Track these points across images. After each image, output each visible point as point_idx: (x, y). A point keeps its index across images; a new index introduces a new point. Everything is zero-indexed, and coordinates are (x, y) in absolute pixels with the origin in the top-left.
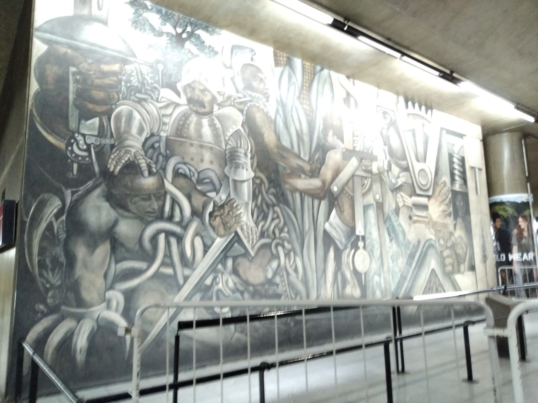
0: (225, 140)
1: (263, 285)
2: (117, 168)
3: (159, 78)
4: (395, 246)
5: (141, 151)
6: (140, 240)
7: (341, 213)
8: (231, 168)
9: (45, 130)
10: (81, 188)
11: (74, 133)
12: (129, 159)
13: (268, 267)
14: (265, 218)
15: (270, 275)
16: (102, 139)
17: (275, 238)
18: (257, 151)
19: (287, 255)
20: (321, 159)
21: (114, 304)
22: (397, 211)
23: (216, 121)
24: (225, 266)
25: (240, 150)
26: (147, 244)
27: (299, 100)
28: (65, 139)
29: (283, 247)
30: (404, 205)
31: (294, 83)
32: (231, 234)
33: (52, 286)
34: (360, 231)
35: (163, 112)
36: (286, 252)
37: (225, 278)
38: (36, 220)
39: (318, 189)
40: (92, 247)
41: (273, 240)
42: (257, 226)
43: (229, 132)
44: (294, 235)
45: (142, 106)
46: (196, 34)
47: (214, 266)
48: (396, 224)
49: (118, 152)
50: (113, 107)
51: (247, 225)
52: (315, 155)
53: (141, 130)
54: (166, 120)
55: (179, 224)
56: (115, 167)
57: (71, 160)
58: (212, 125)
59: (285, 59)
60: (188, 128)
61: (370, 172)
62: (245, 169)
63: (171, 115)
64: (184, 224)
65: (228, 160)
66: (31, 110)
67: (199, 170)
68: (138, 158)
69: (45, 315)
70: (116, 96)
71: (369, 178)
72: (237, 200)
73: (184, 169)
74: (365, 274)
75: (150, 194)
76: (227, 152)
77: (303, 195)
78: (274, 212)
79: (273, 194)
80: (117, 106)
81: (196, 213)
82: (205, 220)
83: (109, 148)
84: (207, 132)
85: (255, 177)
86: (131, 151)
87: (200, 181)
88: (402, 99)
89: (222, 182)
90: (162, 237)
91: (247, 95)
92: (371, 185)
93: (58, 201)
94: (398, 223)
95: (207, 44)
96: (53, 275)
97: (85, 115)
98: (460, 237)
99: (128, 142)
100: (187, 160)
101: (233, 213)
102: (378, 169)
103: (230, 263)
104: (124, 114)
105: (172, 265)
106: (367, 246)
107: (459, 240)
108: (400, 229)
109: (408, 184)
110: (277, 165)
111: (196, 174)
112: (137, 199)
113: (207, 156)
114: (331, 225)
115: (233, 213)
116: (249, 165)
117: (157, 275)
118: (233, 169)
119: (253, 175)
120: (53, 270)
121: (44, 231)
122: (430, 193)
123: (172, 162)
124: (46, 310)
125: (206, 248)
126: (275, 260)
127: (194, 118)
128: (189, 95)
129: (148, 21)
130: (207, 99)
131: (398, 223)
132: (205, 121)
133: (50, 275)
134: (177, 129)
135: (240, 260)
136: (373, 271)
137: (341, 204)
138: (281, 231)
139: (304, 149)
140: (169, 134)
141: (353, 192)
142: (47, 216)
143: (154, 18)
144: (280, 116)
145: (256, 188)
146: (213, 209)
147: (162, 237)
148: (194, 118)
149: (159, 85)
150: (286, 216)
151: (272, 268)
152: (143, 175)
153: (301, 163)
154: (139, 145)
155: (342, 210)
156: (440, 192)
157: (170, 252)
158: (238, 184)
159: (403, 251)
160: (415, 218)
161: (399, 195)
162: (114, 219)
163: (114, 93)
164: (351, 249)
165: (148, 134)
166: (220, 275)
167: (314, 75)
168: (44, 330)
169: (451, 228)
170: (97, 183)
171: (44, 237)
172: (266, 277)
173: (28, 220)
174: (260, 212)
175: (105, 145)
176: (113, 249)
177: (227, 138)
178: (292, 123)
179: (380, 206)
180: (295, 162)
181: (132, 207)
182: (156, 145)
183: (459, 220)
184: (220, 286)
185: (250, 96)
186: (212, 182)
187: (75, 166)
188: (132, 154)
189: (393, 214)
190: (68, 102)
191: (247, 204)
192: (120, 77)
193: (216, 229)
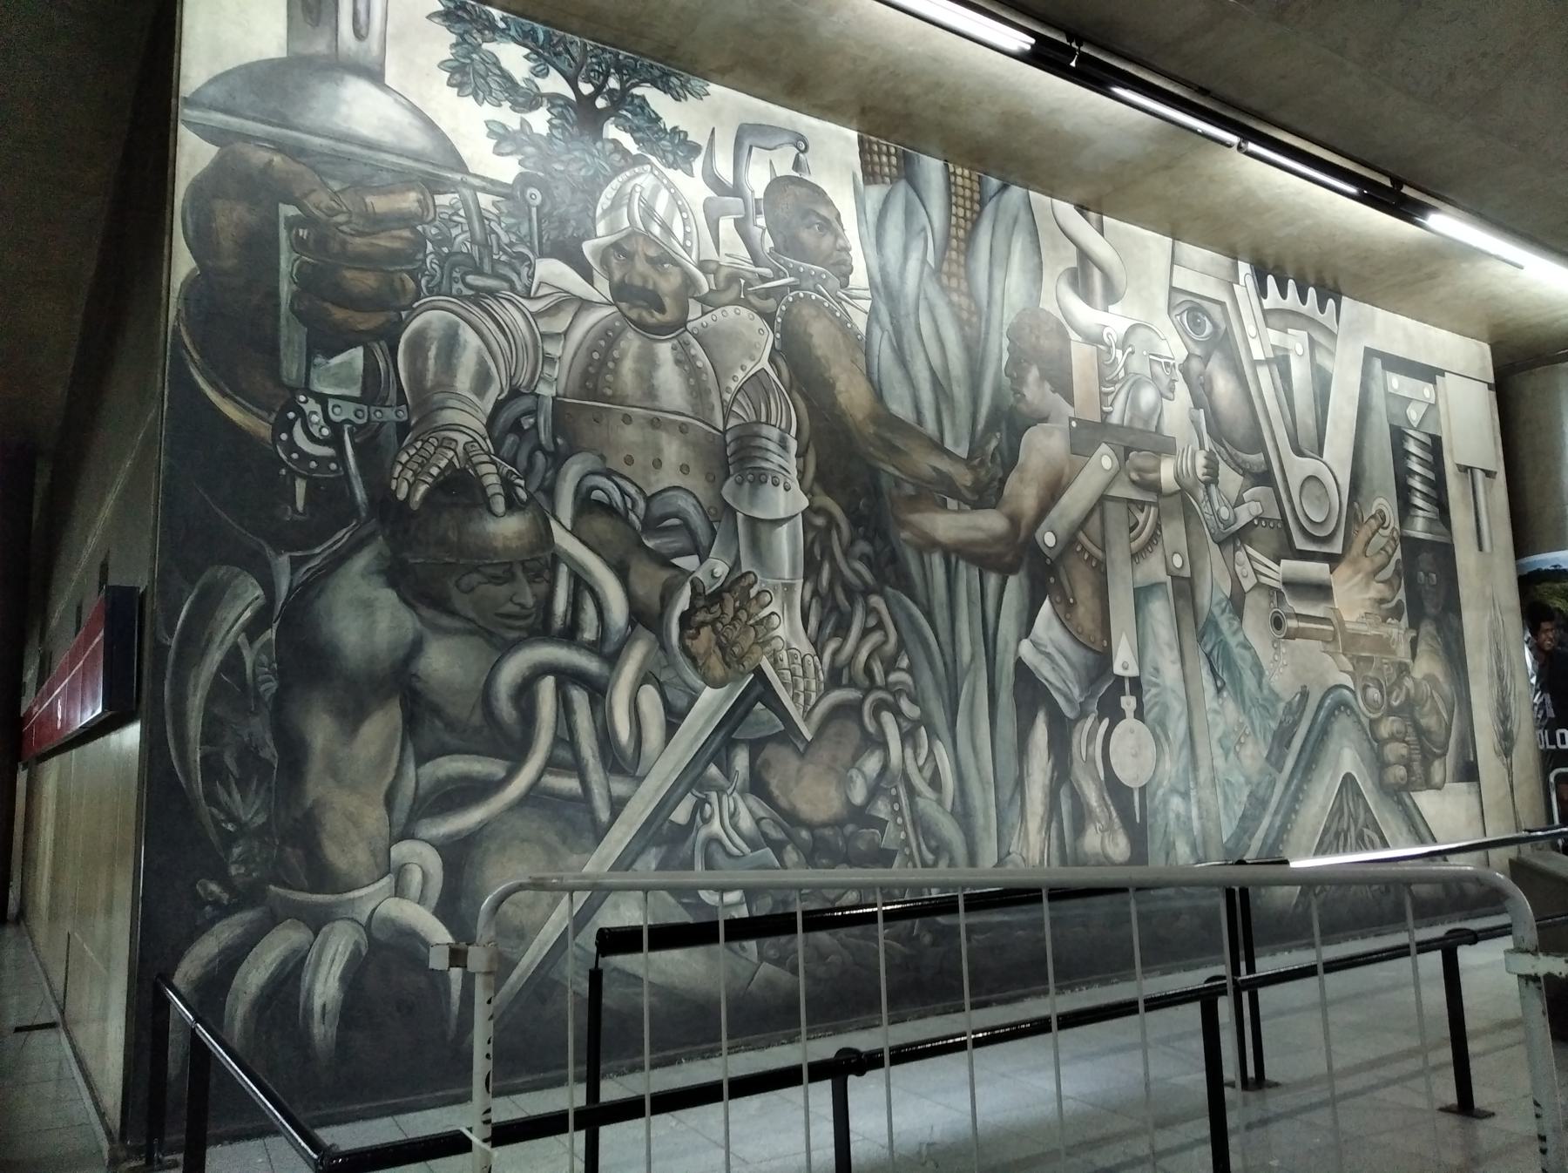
0: (722, 401)
1: (838, 823)
2: (416, 490)
3: (530, 228)
4: (1230, 706)
5: (484, 439)
6: (487, 696)
8: (740, 484)
9: (213, 384)
10: (318, 550)
11: (294, 391)
12: (450, 461)
13: (854, 772)
14: (842, 630)
15: (859, 796)
16: (373, 409)
17: (873, 686)
18: (815, 432)
19: (908, 737)
20: (1006, 454)
21: (415, 877)
22: (1237, 603)
23: (697, 350)
24: (727, 770)
25: (765, 430)
26: (505, 709)
27: (939, 280)
28: (270, 410)
29: (897, 713)
30: (1259, 585)
31: (924, 229)
32: (744, 675)
34: (1124, 661)
35: (544, 326)
38: (194, 640)
39: (998, 539)
40: (352, 717)
41: (867, 692)
42: (820, 655)
44: (926, 678)
46: (633, 96)
47: (699, 769)
48: (1233, 642)
49: (419, 444)
50: (404, 314)
51: (789, 648)
52: (988, 442)
53: (482, 381)
54: (553, 349)
55: (594, 648)
56: (412, 487)
57: (290, 470)
58: (684, 360)
60: (615, 372)
61: (1154, 487)
62: (781, 486)
63: (566, 333)
64: (609, 648)
65: (730, 460)
66: (176, 331)
67: (649, 494)
68: (475, 460)
69: (225, 911)
70: (411, 285)
71: (1150, 504)
72: (759, 577)
73: (606, 490)
74: (1143, 789)
75: (511, 563)
76: (728, 438)
77: (953, 560)
78: (870, 611)
79: (864, 558)
81: (644, 617)
82: (669, 637)
83: (392, 432)
84: (669, 379)
86: (456, 441)
87: (653, 524)
88: (1244, 268)
90: (547, 685)
92: (1158, 526)
93: (255, 587)
94: (1240, 638)
97: (327, 341)
98: (1430, 678)
99: (449, 416)
100: (616, 463)
102: (1177, 478)
103: (741, 760)
104: (435, 333)
105: (577, 767)
106: (1146, 708)
107: (1426, 688)
108: (1247, 655)
109: (1268, 520)
110: (875, 473)
111: (641, 504)
112: (476, 577)
113: (672, 450)
114: (1035, 644)
115: (750, 617)
116: (794, 473)
117: (535, 797)
118: (747, 484)
119: (805, 503)
120: (243, 784)
121: (219, 670)
122: (1336, 548)
123: (573, 472)
124: (225, 897)
125: (674, 718)
126: (872, 752)
127: (632, 343)
128: (617, 276)
129: (497, 64)
130: (668, 284)
131: (1240, 638)
132: (665, 350)
133: (237, 797)
134: (586, 376)
135: (770, 751)
137: (1066, 583)
138: (890, 665)
139: (953, 424)
140: (561, 392)
141: (1104, 551)
142: (226, 627)
143: (513, 58)
144: (883, 330)
145: (813, 543)
146: (691, 603)
147: (547, 685)
148: (632, 343)
150: (904, 625)
151: (864, 776)
153: (944, 465)
154: (477, 424)
155: (1071, 601)
156: (1368, 543)
157: (571, 730)
158: (763, 529)
159: (1257, 723)
160: (1292, 623)
161: (1241, 555)
162: (410, 637)
163: (406, 276)
164: (1100, 719)
165: (502, 390)
166: (714, 796)
167: (982, 203)
168: (221, 953)
169: (1403, 652)
170: (364, 532)
171: (217, 691)
172: (848, 801)
173: (173, 643)
174: (826, 610)
175: (382, 424)
176: (411, 723)
177: (728, 397)
178: (917, 347)
179: (1184, 589)
180: (927, 463)
181: (460, 602)
182: (527, 423)
183: (1427, 628)
185: (794, 272)
186: (686, 526)
187: (301, 487)
188: (460, 449)
189: (1223, 611)
190: (278, 305)
191: (789, 588)
192: (420, 228)
193: (700, 663)
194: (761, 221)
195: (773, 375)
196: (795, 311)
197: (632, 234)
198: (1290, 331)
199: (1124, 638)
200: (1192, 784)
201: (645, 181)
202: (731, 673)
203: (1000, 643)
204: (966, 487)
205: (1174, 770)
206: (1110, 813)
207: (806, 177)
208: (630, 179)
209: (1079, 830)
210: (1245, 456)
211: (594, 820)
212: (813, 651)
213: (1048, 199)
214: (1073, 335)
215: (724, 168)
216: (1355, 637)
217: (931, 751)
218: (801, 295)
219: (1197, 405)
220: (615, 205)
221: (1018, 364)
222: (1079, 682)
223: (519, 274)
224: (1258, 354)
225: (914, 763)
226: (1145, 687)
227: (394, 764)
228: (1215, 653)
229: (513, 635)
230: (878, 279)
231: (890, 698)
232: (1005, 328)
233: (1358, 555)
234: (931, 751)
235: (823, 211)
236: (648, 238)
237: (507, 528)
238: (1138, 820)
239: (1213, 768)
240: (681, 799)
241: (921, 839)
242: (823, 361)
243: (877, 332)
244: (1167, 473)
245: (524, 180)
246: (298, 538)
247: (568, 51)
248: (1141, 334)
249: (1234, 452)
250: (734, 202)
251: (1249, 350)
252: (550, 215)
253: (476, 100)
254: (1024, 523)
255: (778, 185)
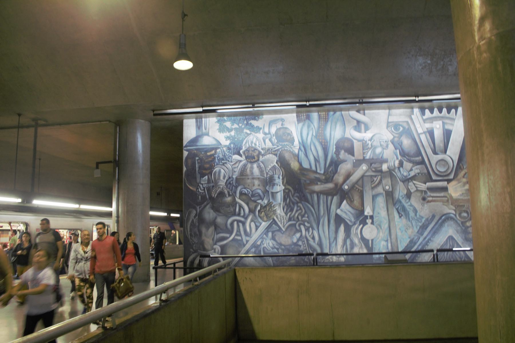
0: (266, 172)
1: (290, 245)
4: (404, 220)
7: (351, 203)
8: (270, 186)
9: (189, 185)
11: (198, 184)
12: (220, 190)
13: (294, 236)
14: (292, 210)
15: (295, 240)
19: (307, 229)
20: (334, 170)
21: (217, 250)
22: (409, 195)
24: (267, 236)
26: (229, 226)
30: (417, 190)
31: (313, 128)
32: (271, 220)
33: (195, 243)
34: (368, 211)
35: (234, 166)
36: (306, 228)
37: (267, 242)
38: (188, 219)
39: (331, 189)
40: (208, 228)
41: (297, 222)
43: (269, 168)
45: (224, 166)
47: (262, 236)
48: (406, 205)
51: (280, 215)
54: (235, 170)
55: (243, 217)
56: (215, 195)
58: (259, 167)
59: (305, 117)
60: (246, 171)
61: (381, 171)
64: (245, 216)
66: (184, 180)
69: (193, 253)
70: (214, 165)
72: (274, 202)
73: (245, 191)
74: (372, 240)
76: (267, 178)
77: (319, 195)
79: (297, 197)
80: (214, 169)
81: (252, 211)
84: (256, 171)
85: (285, 189)
87: (253, 195)
89: (265, 194)
90: (235, 223)
91: (279, 145)
94: (409, 204)
95: (255, 126)
96: (195, 239)
97: (203, 175)
101: (272, 210)
102: (388, 168)
103: (270, 234)
104: (217, 171)
105: (240, 235)
108: (412, 208)
110: (300, 180)
111: (251, 193)
113: (257, 182)
114: (341, 210)
115: (272, 210)
116: (281, 183)
117: (234, 239)
118: (271, 187)
119: (283, 188)
120: (195, 237)
121: (191, 222)
124: (193, 251)
125: (257, 228)
126: (298, 233)
127: (249, 165)
128: (246, 155)
129: (226, 126)
130: (255, 154)
131: (409, 204)
132: (255, 166)
133: (194, 239)
134: (241, 173)
135: (276, 233)
136: (380, 238)
138: (303, 216)
140: (237, 176)
141: (363, 187)
143: (228, 124)
144: (302, 151)
145: (285, 195)
146: (260, 208)
147: (235, 223)
148: (249, 165)
149: (232, 154)
150: (306, 209)
151: (296, 237)
152: (226, 196)
153: (317, 176)
154: (224, 184)
155: (352, 200)
157: (239, 229)
158: (275, 194)
159: (414, 224)
160: (431, 199)
161: (411, 184)
164: (360, 225)
167: (328, 119)
171: (191, 225)
172: (293, 242)
173: (186, 219)
175: (210, 186)
177: (267, 171)
180: (312, 176)
181: (222, 211)
182: (231, 182)
184: (265, 245)
185: (281, 145)
186: (259, 195)
187: (200, 197)
189: (403, 198)
190: (196, 172)
191: (280, 204)
193: (262, 218)
194: (274, 137)
195: (277, 165)
196: (282, 152)
197: (249, 147)
198: (434, 122)
199: (368, 207)
200: (389, 238)
201: (251, 137)
202: (268, 219)
203: (331, 211)
204: (323, 179)
205: (383, 235)
206: (362, 245)
207: (284, 126)
208: (248, 138)
209: (352, 248)
210: (414, 159)
211: (244, 244)
212: (285, 215)
213: (347, 112)
214: (355, 141)
215: (267, 130)
216: (457, 200)
217: (312, 233)
218: (283, 149)
219: (396, 149)
220: (246, 143)
221: (337, 152)
222: (354, 217)
223: (230, 159)
224: (420, 131)
225: (308, 235)
226: (374, 217)
227: (213, 235)
228: (400, 208)
229: (230, 215)
230: (301, 141)
231: (303, 223)
232: (334, 144)
233: (460, 178)
234: (312, 233)
235: (288, 132)
236: (252, 147)
237: (229, 199)
238: (370, 246)
239: (396, 235)
240: (259, 240)
241: (310, 249)
242: (288, 160)
243: (300, 152)
244: (385, 167)
245: (230, 144)
246: (200, 204)
247: (237, 120)
248: (377, 136)
249: (409, 158)
250: (269, 136)
251: (417, 131)
252: (235, 148)
253: (223, 133)
254: (339, 185)
255: (278, 130)
